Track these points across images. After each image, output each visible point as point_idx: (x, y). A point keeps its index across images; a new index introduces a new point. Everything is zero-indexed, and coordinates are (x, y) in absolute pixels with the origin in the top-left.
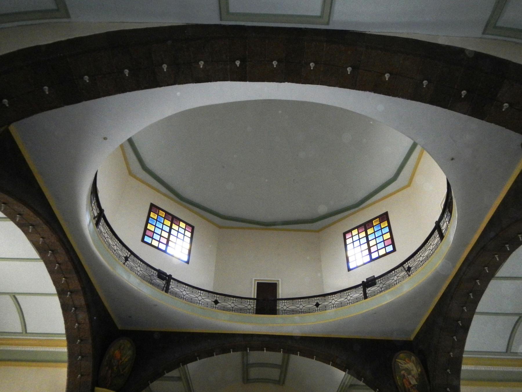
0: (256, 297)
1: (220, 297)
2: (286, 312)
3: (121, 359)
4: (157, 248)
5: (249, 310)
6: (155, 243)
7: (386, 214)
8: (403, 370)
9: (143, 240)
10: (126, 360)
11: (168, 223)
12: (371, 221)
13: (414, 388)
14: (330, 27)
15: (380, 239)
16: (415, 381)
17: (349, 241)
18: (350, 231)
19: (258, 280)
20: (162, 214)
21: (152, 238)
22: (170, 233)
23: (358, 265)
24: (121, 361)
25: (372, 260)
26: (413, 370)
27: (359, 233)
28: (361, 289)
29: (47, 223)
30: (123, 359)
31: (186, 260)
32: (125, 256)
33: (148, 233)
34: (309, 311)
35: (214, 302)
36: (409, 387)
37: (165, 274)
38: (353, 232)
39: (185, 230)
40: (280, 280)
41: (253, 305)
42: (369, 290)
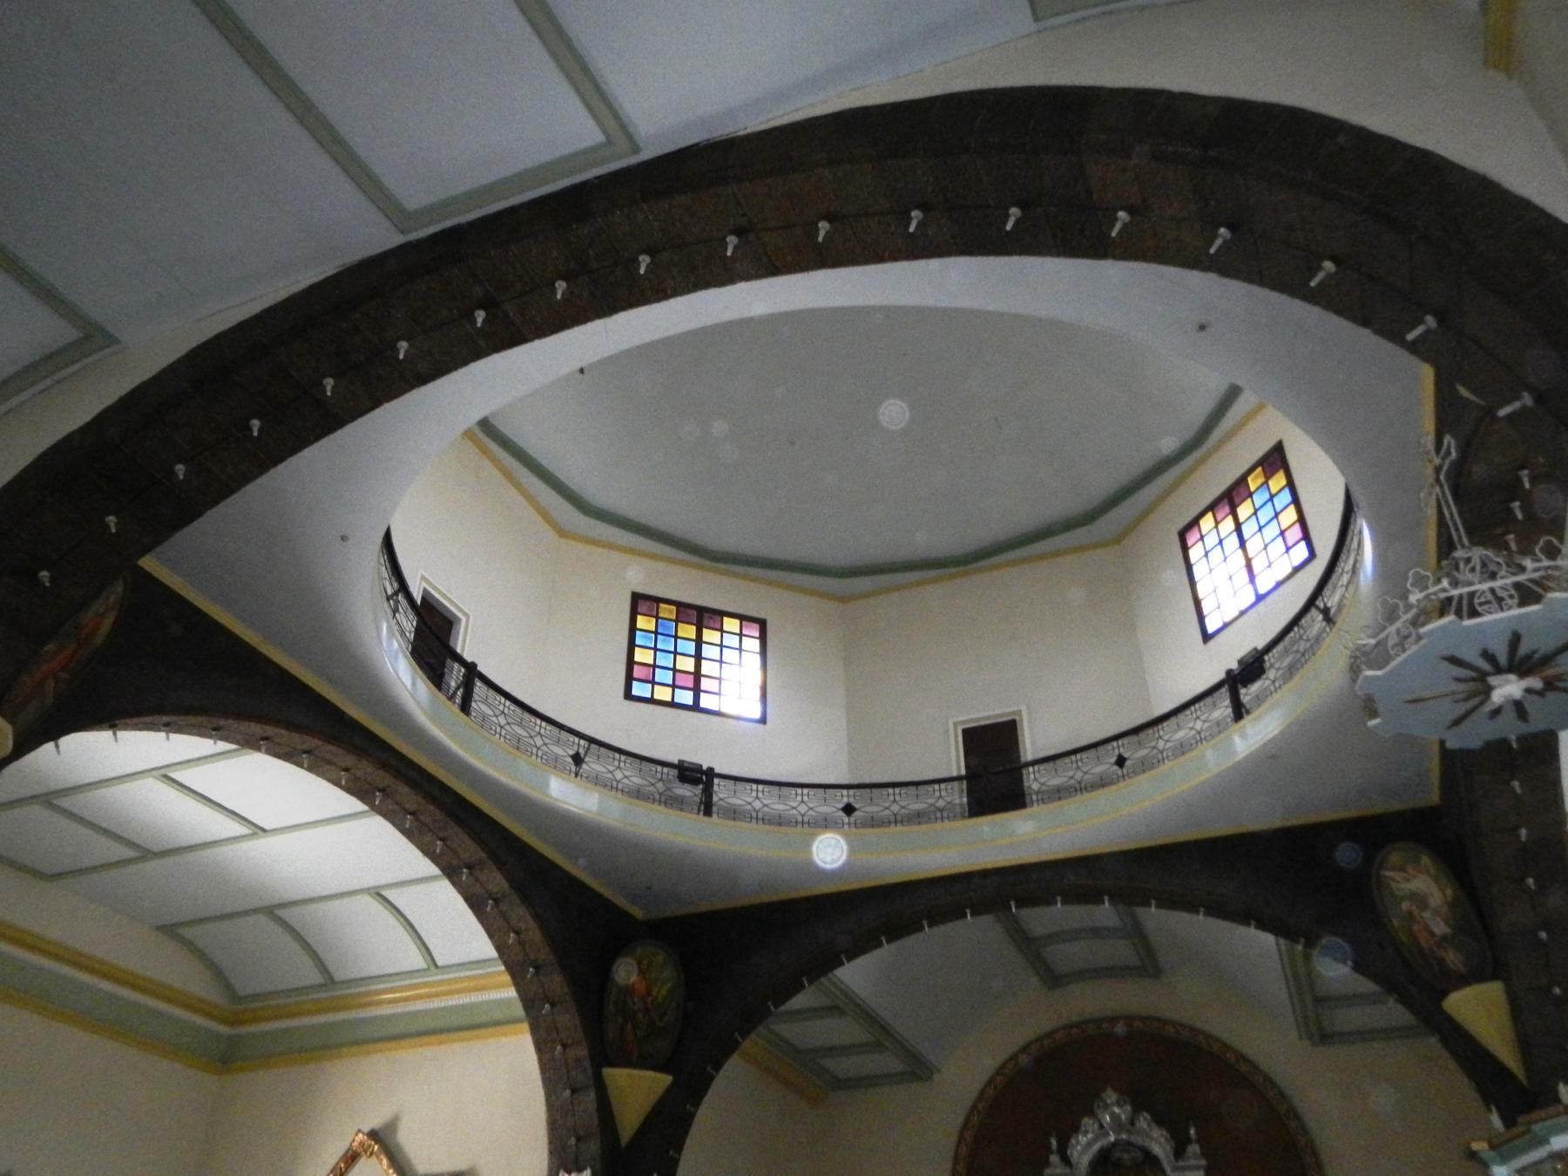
0: (963, 772)
1: (858, 792)
2: (1059, 793)
3: (649, 993)
4: (672, 704)
5: (941, 810)
6: (663, 694)
7: (1279, 449)
8: (1403, 898)
9: (628, 695)
10: (664, 992)
11: (689, 631)
12: (1242, 480)
14: (647, 154)
15: (1272, 531)
16: (1442, 924)
17: (1195, 553)
18: (1195, 523)
19: (963, 722)
20: (668, 611)
21: (653, 683)
22: (698, 657)
23: (1227, 620)
24: (649, 1000)
25: (1260, 598)
27: (1217, 523)
28: (1224, 690)
29: (332, 739)
31: (757, 715)
32: (572, 753)
33: (638, 672)
34: (1102, 783)
37: (697, 769)
38: (1202, 522)
39: (741, 635)
40: (1023, 708)
41: (957, 796)
42: (1247, 694)
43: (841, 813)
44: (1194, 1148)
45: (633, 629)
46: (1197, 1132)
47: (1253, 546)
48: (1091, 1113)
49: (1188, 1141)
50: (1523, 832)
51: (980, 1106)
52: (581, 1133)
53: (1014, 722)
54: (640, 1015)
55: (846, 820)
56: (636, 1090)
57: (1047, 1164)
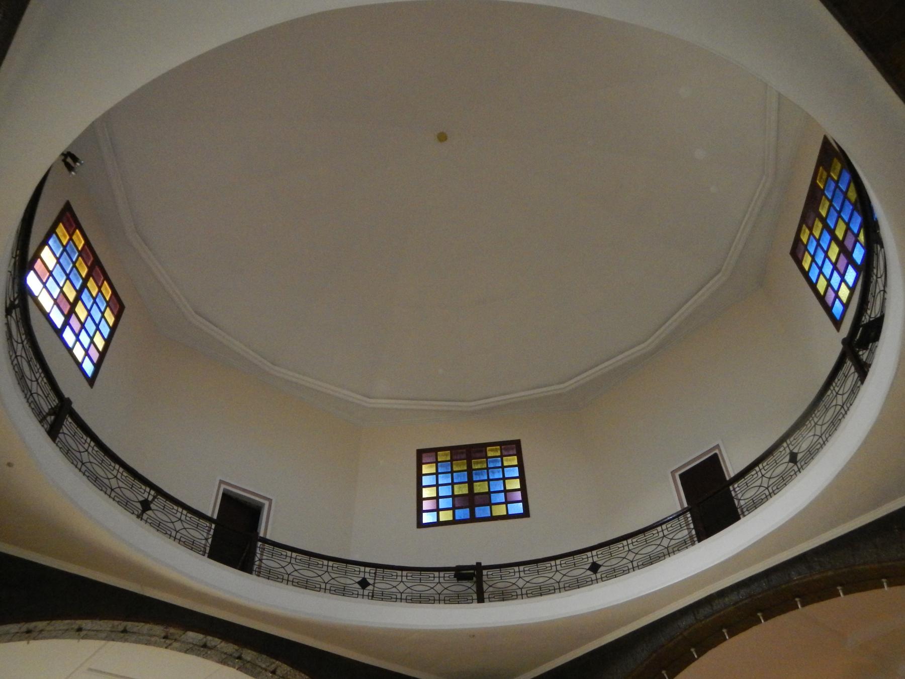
1: (599, 551)
20: (443, 456)
43: (589, 573)
45: (420, 475)
47: (840, 233)
53: (716, 455)
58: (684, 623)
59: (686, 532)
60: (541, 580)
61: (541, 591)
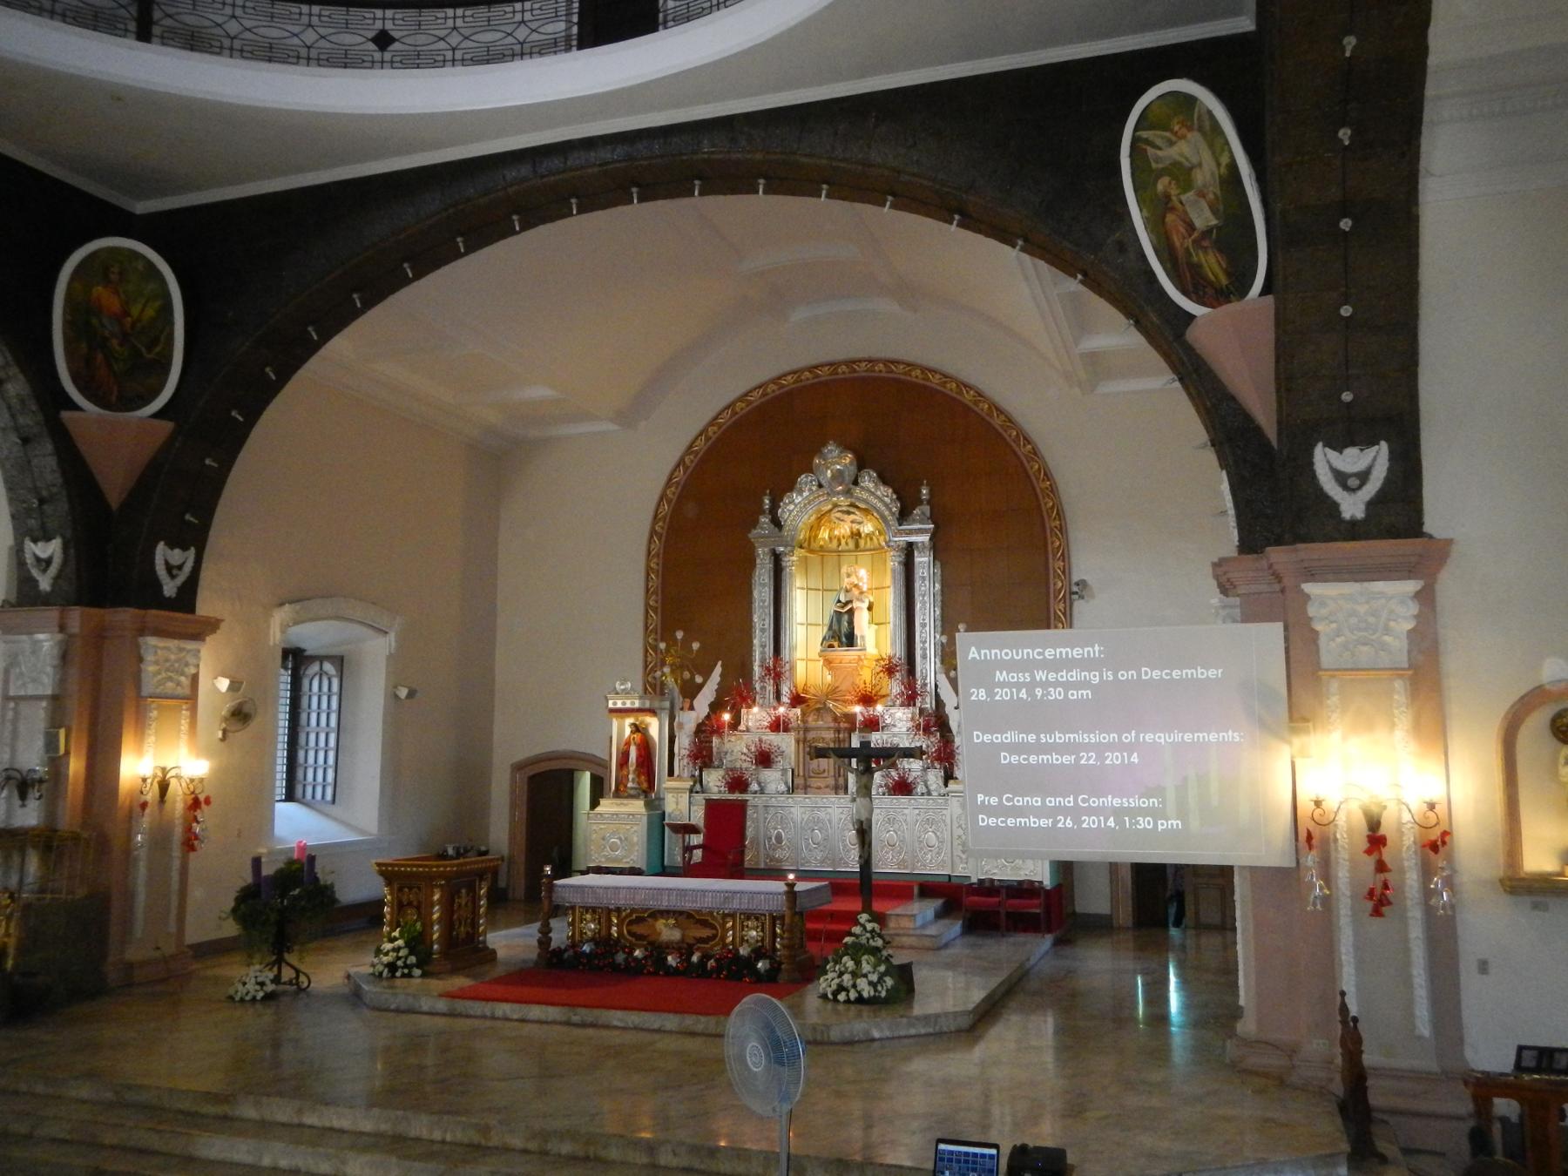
3: (126, 313)
13: (1206, 243)
16: (1208, 213)
26: (1200, 165)
30: (135, 311)
35: (393, 40)
36: (1189, 242)
43: (372, 46)
44: (927, 509)
46: (931, 492)
48: (809, 469)
49: (920, 502)
50: (1350, 42)
51: (687, 460)
52: (45, 493)
54: (115, 342)
55: (377, 56)
56: (122, 439)
57: (755, 523)
58: (511, 174)
59: (562, 26)
60: (275, 33)
61: (270, 53)
